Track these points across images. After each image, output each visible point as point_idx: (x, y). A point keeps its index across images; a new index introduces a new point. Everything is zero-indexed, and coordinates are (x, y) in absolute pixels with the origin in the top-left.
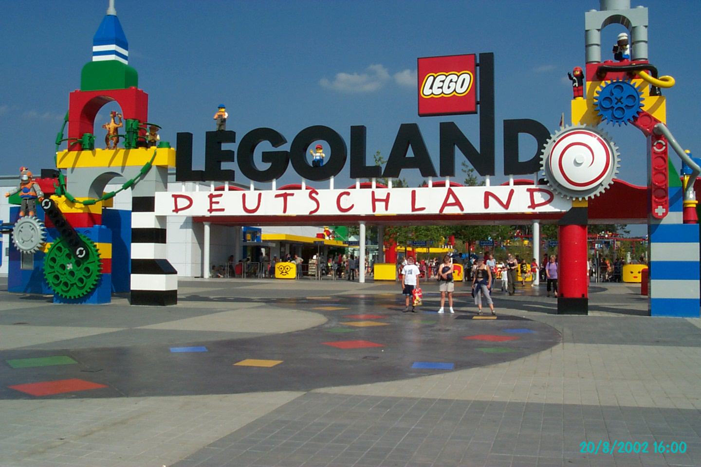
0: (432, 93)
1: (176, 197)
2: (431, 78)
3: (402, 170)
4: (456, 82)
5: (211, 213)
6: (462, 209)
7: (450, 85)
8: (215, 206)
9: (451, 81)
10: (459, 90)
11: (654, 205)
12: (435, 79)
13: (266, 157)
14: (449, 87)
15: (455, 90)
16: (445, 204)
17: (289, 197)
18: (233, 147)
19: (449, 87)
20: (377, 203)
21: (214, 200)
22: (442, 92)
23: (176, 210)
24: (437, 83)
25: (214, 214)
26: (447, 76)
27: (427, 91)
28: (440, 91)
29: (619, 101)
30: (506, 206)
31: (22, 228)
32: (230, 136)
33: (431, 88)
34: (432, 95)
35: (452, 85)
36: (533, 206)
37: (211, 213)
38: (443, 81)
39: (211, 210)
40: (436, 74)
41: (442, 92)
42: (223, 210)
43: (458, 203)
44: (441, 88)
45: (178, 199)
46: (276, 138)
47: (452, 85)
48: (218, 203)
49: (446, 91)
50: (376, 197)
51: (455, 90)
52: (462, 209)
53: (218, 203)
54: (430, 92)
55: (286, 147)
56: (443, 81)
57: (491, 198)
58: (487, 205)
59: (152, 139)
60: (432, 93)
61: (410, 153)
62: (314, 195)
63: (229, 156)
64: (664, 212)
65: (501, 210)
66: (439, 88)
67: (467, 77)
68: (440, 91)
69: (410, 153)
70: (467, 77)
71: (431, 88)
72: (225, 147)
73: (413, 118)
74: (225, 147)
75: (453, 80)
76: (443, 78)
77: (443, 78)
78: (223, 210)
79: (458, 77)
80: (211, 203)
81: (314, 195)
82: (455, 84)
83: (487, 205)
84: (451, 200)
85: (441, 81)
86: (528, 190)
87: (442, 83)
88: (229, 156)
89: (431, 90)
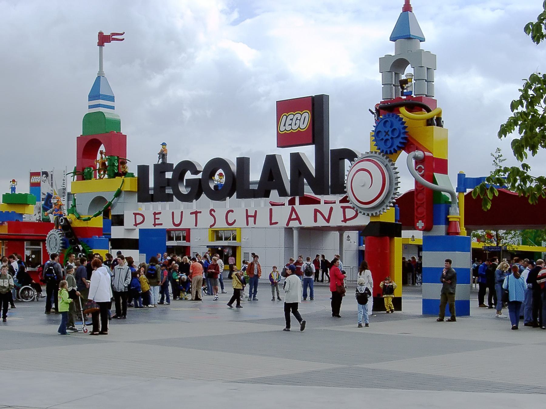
1: (135, 214)
4: (300, 120)
5: (155, 226)
6: (300, 223)
8: (157, 222)
9: (297, 119)
11: (416, 220)
12: (287, 117)
13: (190, 183)
14: (296, 124)
15: (299, 127)
16: (290, 219)
17: (198, 214)
19: (296, 124)
20: (249, 218)
21: (157, 216)
23: (136, 225)
25: (157, 227)
29: (387, 133)
30: (328, 221)
31: (51, 238)
32: (169, 167)
33: (285, 125)
36: (345, 220)
37: (155, 226)
38: (292, 120)
39: (155, 225)
42: (161, 224)
43: (298, 219)
44: (291, 125)
45: (137, 216)
47: (298, 122)
48: (158, 219)
50: (249, 214)
52: (300, 223)
53: (158, 219)
55: (200, 176)
56: (292, 120)
57: (319, 215)
58: (316, 220)
59: (124, 170)
62: (212, 212)
64: (419, 228)
65: (325, 224)
66: (289, 125)
67: (306, 115)
70: (306, 115)
71: (285, 125)
73: (272, 149)
78: (161, 224)
79: (301, 115)
80: (155, 219)
81: (212, 212)
82: (299, 121)
83: (316, 220)
84: (294, 216)
86: (342, 207)
87: (291, 121)
89: (284, 127)
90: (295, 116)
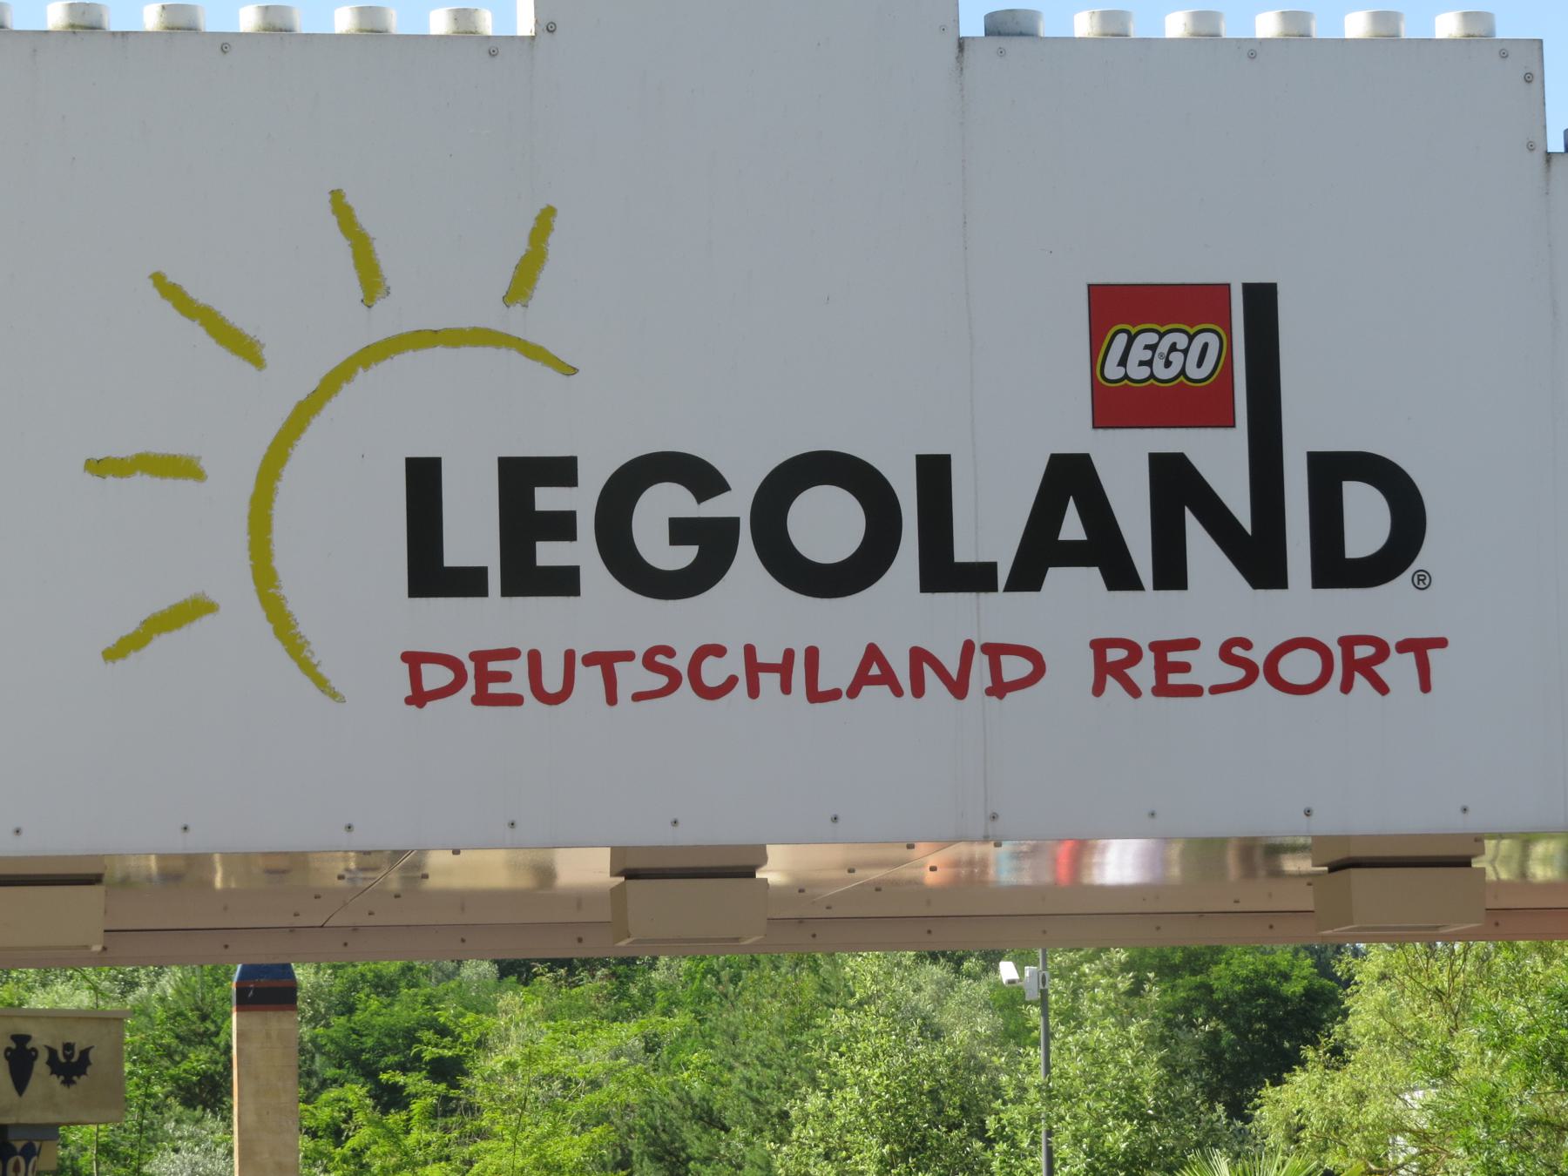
0: (1126, 377)
2: (1122, 339)
3: (1052, 571)
4: (1185, 352)
7: (1171, 358)
9: (1173, 348)
10: (1194, 372)
13: (681, 531)
14: (1168, 364)
15: (1183, 372)
18: (581, 500)
22: (1152, 376)
24: (1138, 353)
26: (1162, 335)
27: (1113, 371)
28: (1144, 372)
33: (1123, 362)
34: (1126, 381)
35: (1177, 358)
40: (1134, 326)
41: (1152, 376)
44: (1149, 363)
46: (704, 479)
47: (1177, 358)
49: (1161, 372)
51: (1183, 372)
54: (1119, 373)
56: (1152, 348)
60: (1126, 377)
61: (1072, 528)
63: (563, 526)
66: (1142, 363)
68: (1144, 372)
69: (1072, 528)
71: (1123, 362)
72: (547, 499)
73: (1078, 436)
74: (547, 499)
75: (1178, 347)
76: (1152, 338)
77: (1152, 338)
79: (1191, 338)
82: (1181, 355)
85: (1147, 347)
88: (563, 526)
89: (1122, 369)
90: (1163, 339)
